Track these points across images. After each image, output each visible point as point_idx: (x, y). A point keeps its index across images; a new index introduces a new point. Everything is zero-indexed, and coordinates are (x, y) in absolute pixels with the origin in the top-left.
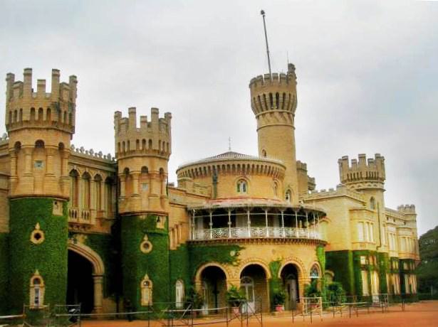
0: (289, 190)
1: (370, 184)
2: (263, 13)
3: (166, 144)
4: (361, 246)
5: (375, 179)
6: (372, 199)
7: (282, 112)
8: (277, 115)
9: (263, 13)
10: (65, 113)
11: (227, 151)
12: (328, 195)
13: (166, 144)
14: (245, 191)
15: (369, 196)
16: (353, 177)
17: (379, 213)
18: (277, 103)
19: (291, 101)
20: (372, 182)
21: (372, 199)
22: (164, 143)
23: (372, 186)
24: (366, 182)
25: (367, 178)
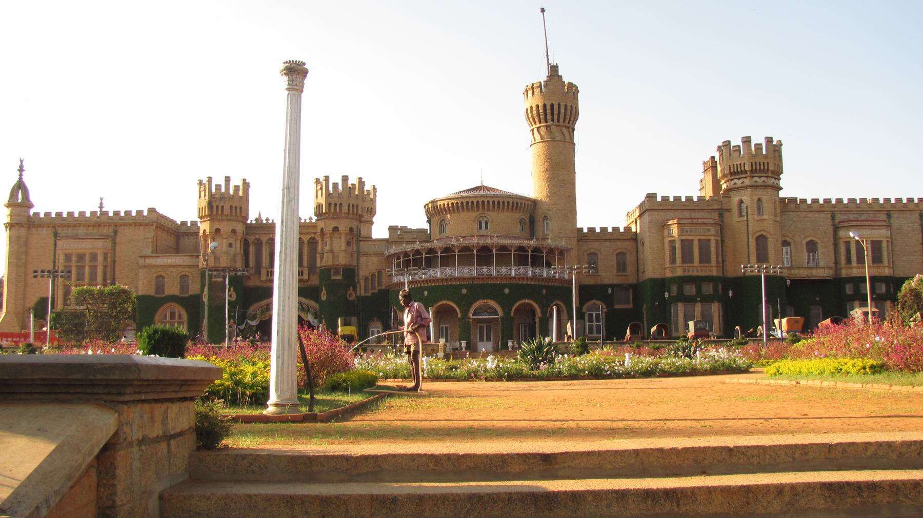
0: (545, 216)
1: (736, 181)
2: (543, 10)
3: (338, 205)
4: (684, 271)
5: (742, 172)
6: (741, 202)
7: (540, 127)
8: (535, 131)
9: (543, 10)
10: (217, 207)
11: (480, 185)
12: (685, 205)
13: (338, 205)
14: (486, 228)
15: (735, 200)
16: (762, 168)
17: (747, 220)
18: (552, 114)
19: (562, 111)
20: (739, 179)
21: (741, 202)
22: (335, 204)
23: (739, 183)
24: (732, 180)
25: (731, 174)
